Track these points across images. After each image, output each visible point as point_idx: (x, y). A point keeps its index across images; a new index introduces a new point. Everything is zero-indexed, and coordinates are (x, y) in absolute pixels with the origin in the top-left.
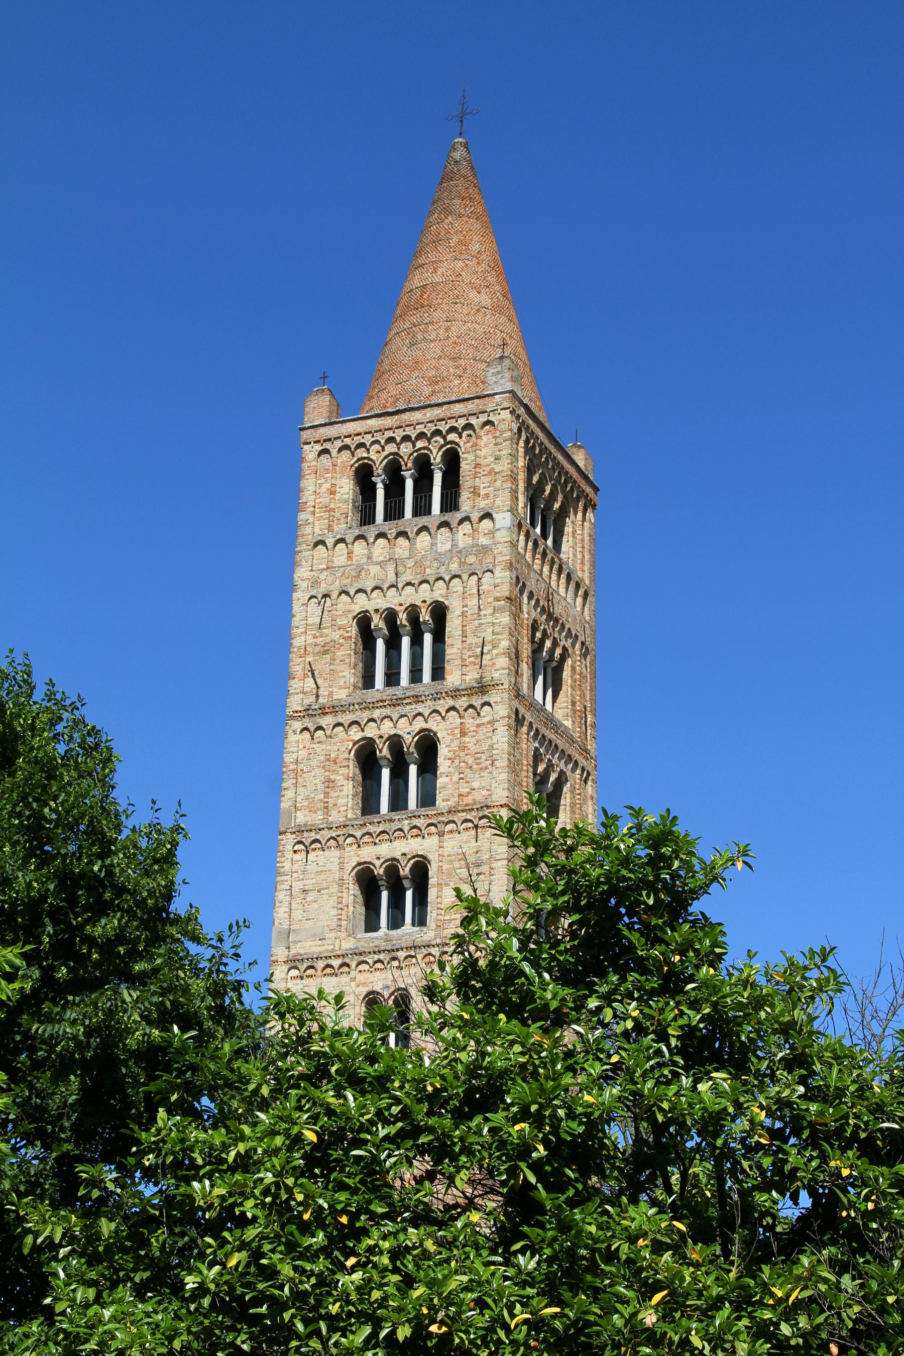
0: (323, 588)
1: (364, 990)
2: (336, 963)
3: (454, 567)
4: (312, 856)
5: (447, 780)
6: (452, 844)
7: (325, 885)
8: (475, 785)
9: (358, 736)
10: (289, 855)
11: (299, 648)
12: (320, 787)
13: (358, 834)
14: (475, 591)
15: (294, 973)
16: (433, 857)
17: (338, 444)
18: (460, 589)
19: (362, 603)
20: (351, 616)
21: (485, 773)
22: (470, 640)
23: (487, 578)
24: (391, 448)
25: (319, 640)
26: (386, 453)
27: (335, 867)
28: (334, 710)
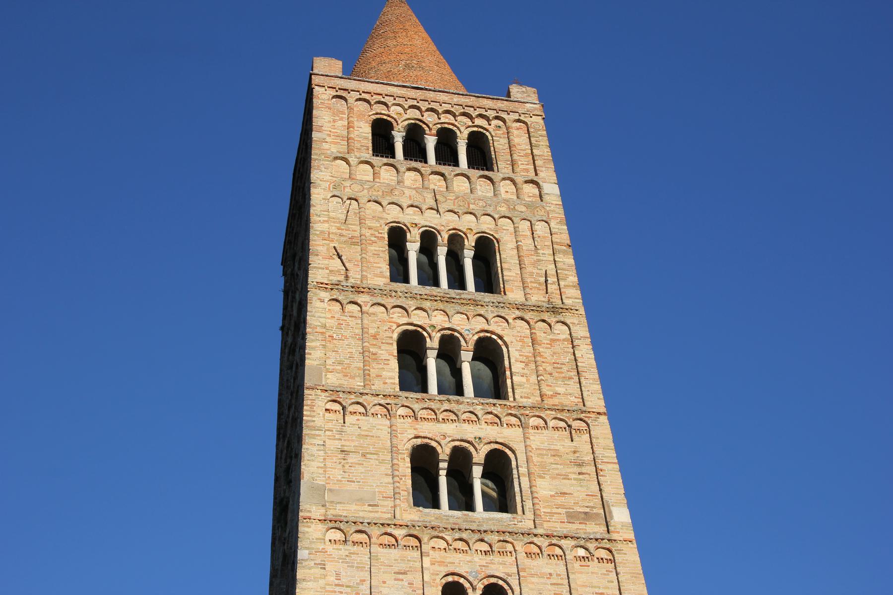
0: (348, 192)
1: (444, 570)
2: (399, 533)
3: (503, 210)
4: (350, 419)
5: (524, 380)
6: (538, 439)
7: (371, 449)
8: (561, 390)
9: (405, 320)
10: (322, 412)
11: (322, 232)
12: (356, 355)
13: (416, 407)
14: (529, 233)
15: (338, 535)
16: (519, 448)
17: (356, 95)
18: (512, 229)
19: (394, 215)
20: (382, 222)
21: (571, 382)
22: (529, 269)
23: (540, 228)
24: (416, 114)
25: (344, 232)
26: (407, 116)
27: (384, 433)
28: (370, 291)
